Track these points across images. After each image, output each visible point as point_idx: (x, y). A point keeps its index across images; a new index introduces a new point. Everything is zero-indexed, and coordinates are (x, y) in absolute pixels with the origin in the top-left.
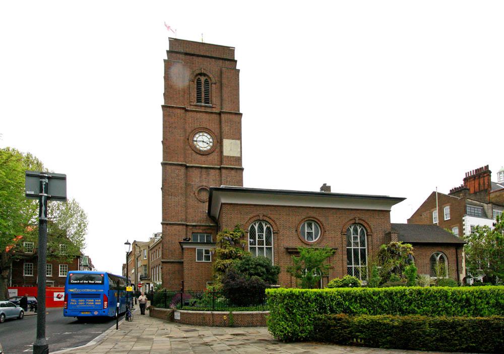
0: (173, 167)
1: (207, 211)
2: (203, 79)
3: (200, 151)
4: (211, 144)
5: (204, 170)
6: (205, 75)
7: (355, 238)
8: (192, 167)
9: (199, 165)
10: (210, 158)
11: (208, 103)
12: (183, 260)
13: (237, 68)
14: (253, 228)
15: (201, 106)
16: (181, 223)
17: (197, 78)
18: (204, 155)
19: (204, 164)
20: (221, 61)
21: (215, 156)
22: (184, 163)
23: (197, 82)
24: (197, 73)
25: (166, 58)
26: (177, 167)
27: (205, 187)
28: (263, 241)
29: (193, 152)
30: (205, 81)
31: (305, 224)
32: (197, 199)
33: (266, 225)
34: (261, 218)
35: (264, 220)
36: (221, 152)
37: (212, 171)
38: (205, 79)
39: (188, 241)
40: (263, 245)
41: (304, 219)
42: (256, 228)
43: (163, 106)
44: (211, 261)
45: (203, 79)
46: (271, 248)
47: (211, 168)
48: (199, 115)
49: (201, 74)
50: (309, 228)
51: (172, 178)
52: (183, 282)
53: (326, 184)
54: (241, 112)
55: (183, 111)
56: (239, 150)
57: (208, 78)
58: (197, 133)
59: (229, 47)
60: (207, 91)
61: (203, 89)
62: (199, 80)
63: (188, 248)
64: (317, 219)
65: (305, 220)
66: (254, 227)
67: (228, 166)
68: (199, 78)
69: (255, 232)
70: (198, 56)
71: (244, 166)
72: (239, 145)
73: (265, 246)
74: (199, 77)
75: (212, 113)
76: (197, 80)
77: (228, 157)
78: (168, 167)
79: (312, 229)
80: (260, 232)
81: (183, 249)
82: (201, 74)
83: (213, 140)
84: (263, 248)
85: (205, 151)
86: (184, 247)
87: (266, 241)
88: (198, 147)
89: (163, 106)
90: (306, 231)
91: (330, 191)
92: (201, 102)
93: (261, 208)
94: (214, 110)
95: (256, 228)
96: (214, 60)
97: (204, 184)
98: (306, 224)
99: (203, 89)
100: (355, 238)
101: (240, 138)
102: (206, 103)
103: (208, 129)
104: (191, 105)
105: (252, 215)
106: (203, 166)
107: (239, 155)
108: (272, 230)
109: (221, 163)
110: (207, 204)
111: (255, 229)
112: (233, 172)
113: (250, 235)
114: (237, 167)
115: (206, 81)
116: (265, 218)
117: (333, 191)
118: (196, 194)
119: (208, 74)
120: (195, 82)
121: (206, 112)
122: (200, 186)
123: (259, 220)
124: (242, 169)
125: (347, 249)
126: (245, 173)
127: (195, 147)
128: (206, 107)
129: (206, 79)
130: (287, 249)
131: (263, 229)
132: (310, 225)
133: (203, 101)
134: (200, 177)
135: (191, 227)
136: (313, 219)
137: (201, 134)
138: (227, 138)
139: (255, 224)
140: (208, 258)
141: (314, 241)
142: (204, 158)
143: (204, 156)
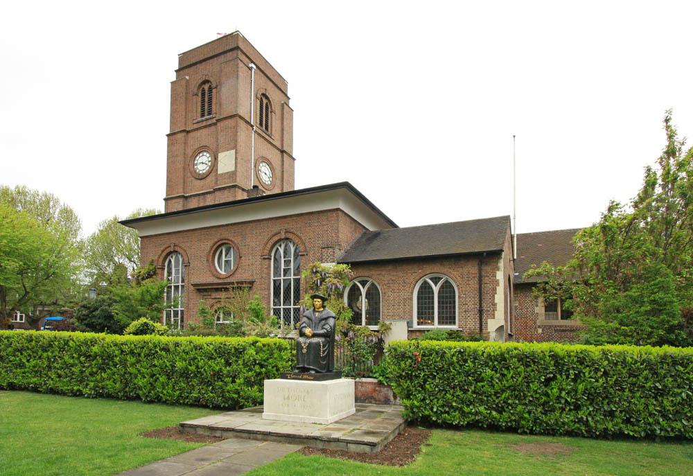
2: (206, 87)
4: (210, 164)
5: (202, 197)
7: (287, 263)
8: (190, 197)
10: (209, 179)
20: (223, 56)
21: (211, 178)
22: (183, 194)
37: (208, 196)
55: (184, 134)
58: (197, 156)
74: (203, 86)
93: (174, 236)
100: (287, 263)
109: (216, 183)
112: (226, 192)
115: (210, 89)
137: (201, 155)
139: (280, 246)
143: (202, 181)
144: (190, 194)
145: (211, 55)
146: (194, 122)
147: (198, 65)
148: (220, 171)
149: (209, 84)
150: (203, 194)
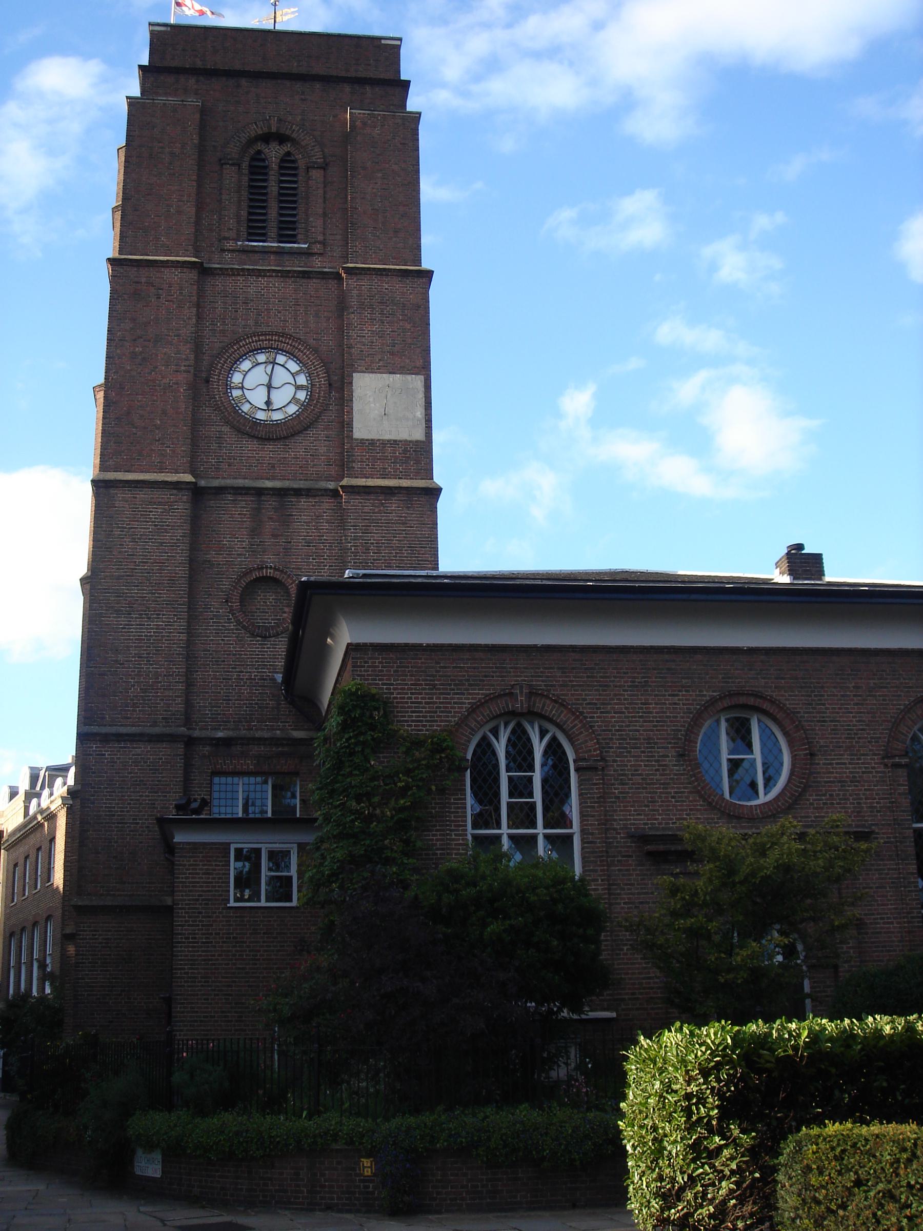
0: (142, 495)
1: (279, 677)
2: (274, 153)
3: (256, 423)
6: (282, 139)
8: (220, 491)
9: (248, 483)
10: (299, 448)
11: (292, 239)
12: (169, 901)
13: (403, 77)
14: (485, 749)
15: (265, 252)
16: (167, 730)
17: (252, 151)
18: (269, 439)
19: (273, 478)
20: (347, 88)
23: (250, 166)
24: (253, 134)
25: (136, 92)
26: (158, 495)
27: (270, 572)
28: (533, 806)
29: (226, 429)
30: (282, 160)
31: (718, 722)
32: (239, 623)
33: (543, 733)
34: (520, 703)
35: (532, 715)
36: (345, 424)
37: (303, 502)
38: (282, 152)
39: (197, 811)
40: (533, 825)
41: (713, 702)
42: (501, 748)
43: (110, 261)
44: (294, 903)
45: (274, 153)
46: (570, 837)
47: (298, 492)
48: (254, 287)
49: (267, 138)
50: (739, 741)
51: (134, 540)
52: (168, 1001)
53: (800, 547)
54: (426, 265)
56: (420, 413)
57: (292, 150)
59: (380, 38)
60: (288, 199)
61: (273, 188)
62: (258, 157)
63: (195, 847)
64: (772, 702)
65: (720, 705)
66: (490, 745)
67: (371, 482)
68: (259, 152)
69: (496, 766)
70: (257, 76)
71: (439, 477)
72: (421, 395)
73: (540, 830)
74: (260, 146)
75: (306, 275)
76: (253, 159)
77: (372, 442)
78: (120, 495)
79: (749, 745)
80: (520, 769)
81: (170, 848)
82: (267, 138)
83: (310, 376)
84: (534, 837)
85: (277, 424)
86: (179, 838)
87: (546, 809)
88: (246, 408)
89: (110, 261)
90: (725, 756)
91: (821, 573)
92: (263, 237)
94: (318, 264)
95: (501, 748)
96: (318, 85)
97: (270, 559)
98: (723, 725)
99: (273, 188)
101: (424, 369)
102: (281, 238)
103: (291, 337)
104: (223, 250)
105: (479, 694)
106: (269, 484)
107: (419, 435)
108: (571, 756)
110: (281, 646)
111: (494, 753)
112: (394, 505)
113: (473, 780)
114: (405, 483)
116: (538, 705)
117: (834, 574)
118: (236, 605)
119: (294, 135)
120: (245, 165)
121: (285, 275)
122: (251, 571)
123: (513, 714)
124: (435, 492)
125: (916, 830)
126: (443, 505)
127: (236, 411)
128: (280, 253)
129: (288, 154)
130: (643, 839)
131: (531, 752)
132: (741, 734)
133: (273, 232)
134: (255, 532)
135: (207, 749)
136: (751, 701)
137: (261, 358)
138: (369, 370)
140: (281, 888)
141: (763, 798)
142: (269, 452)
144: (216, 483)
145: (295, 67)
146: (230, 245)
147: (243, 82)
148: (360, 431)
149: (287, 147)
150: (281, 493)
